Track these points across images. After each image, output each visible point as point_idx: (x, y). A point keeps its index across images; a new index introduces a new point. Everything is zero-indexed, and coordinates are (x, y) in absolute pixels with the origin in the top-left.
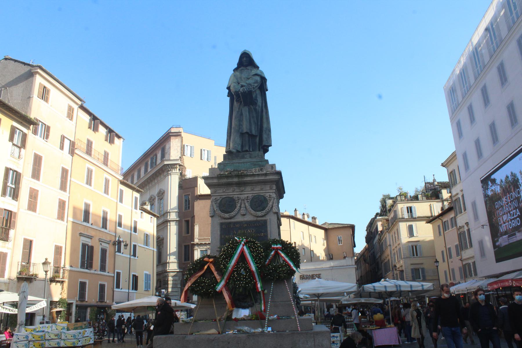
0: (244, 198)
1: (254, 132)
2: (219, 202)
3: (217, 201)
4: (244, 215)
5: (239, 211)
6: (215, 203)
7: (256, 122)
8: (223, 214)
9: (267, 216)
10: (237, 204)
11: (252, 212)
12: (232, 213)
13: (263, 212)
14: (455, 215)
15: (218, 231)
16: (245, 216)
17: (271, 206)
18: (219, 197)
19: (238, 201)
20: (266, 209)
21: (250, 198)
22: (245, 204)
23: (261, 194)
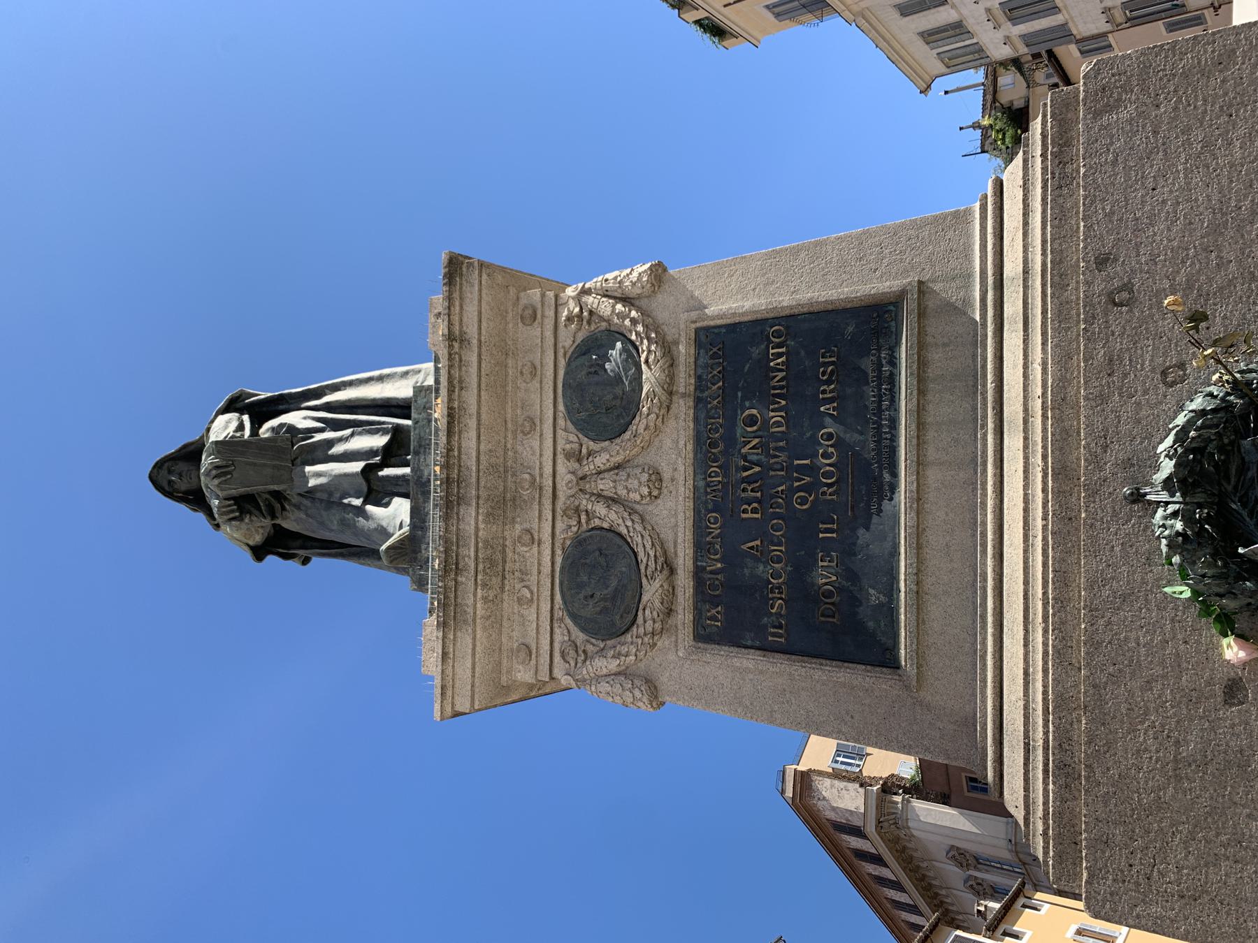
0: (570, 476)
1: (380, 441)
2: (580, 636)
3: (577, 651)
4: (656, 477)
5: (632, 512)
6: (585, 661)
7: (348, 431)
8: (640, 620)
9: (671, 334)
10: (597, 522)
11: (642, 426)
12: (641, 555)
13: (643, 359)
14: (1070, 42)
15: (737, 662)
16: (666, 476)
17: (619, 307)
18: (557, 631)
19: (583, 517)
20: (633, 337)
21: (573, 438)
22: (599, 473)
23: (561, 373)
